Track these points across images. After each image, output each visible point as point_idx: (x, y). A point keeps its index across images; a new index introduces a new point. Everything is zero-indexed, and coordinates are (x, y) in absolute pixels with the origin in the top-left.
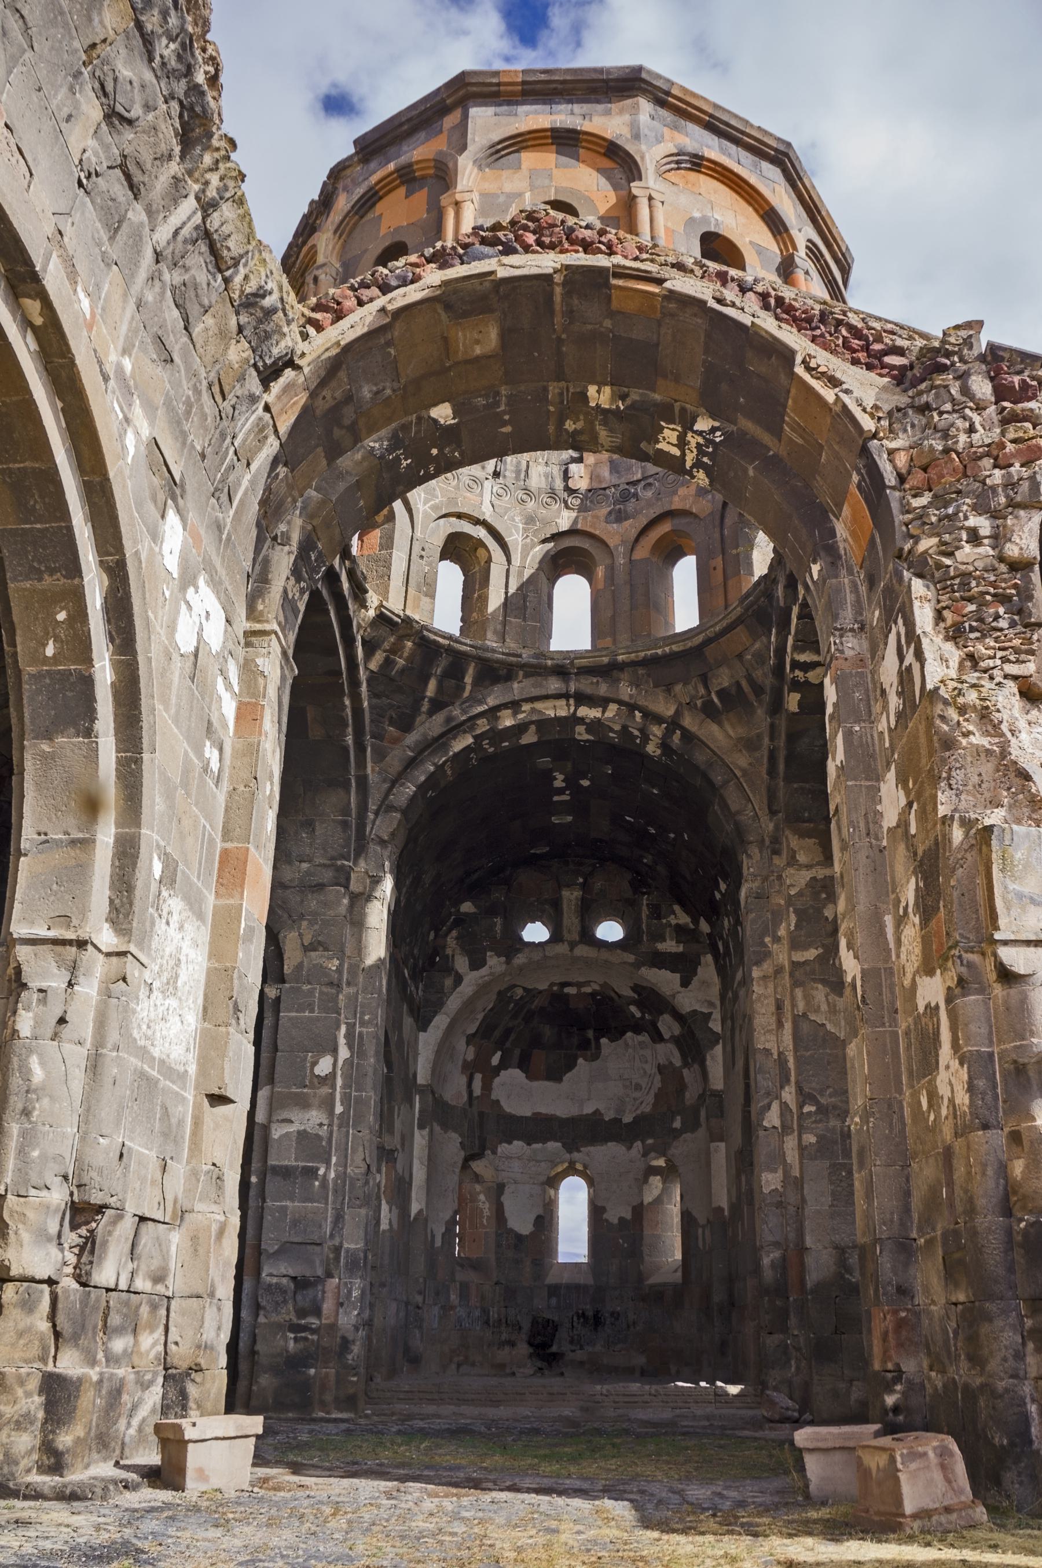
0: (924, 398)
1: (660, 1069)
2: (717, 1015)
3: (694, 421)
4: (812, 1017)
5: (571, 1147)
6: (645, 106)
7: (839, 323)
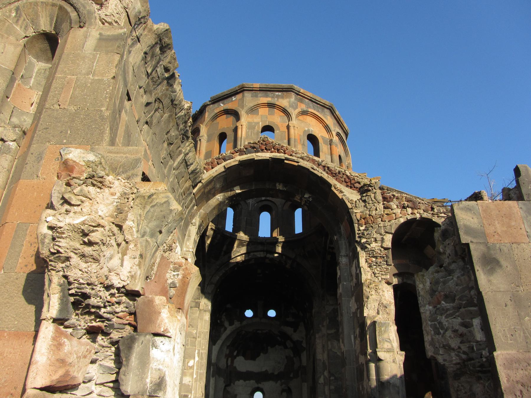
0: (364, 198)
1: (287, 357)
2: (304, 342)
3: (304, 194)
4: (333, 350)
5: (258, 382)
6: (293, 95)
7: (343, 174)
